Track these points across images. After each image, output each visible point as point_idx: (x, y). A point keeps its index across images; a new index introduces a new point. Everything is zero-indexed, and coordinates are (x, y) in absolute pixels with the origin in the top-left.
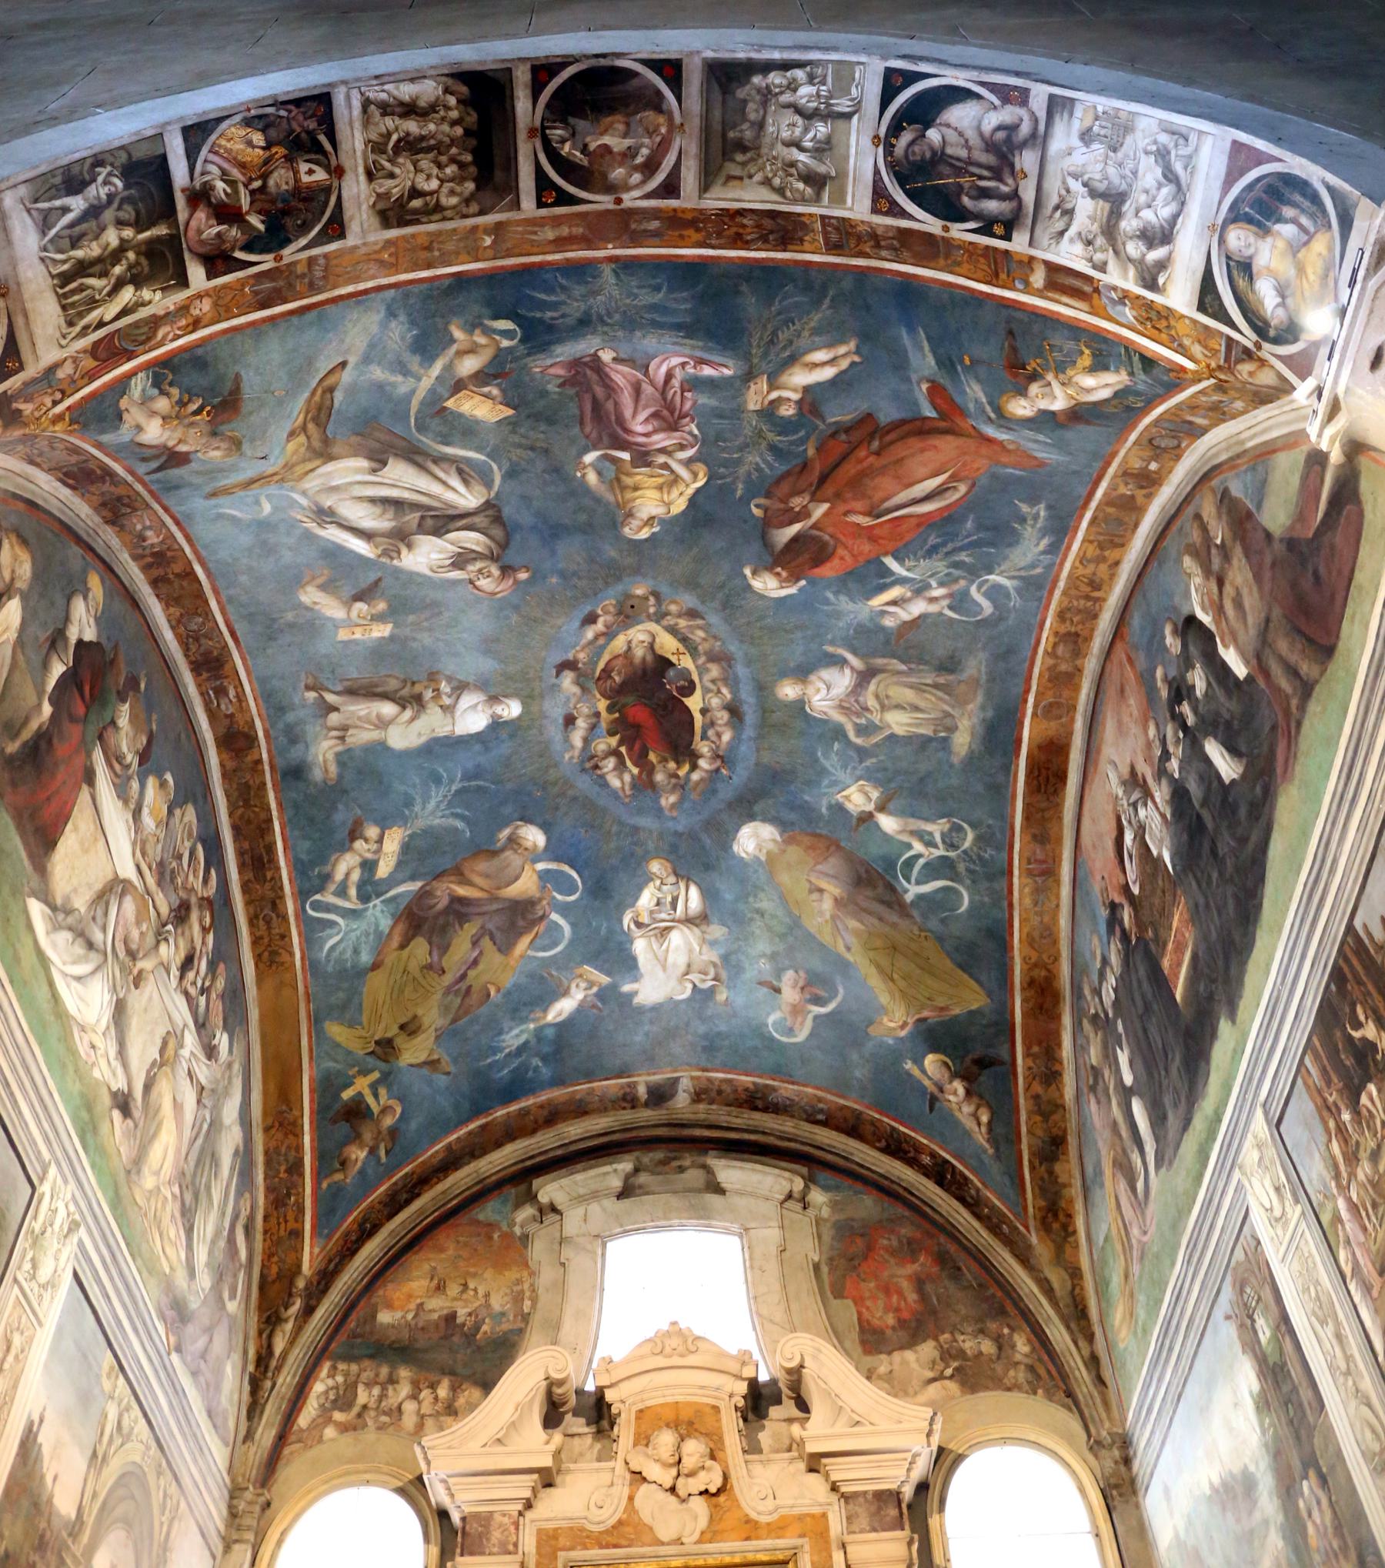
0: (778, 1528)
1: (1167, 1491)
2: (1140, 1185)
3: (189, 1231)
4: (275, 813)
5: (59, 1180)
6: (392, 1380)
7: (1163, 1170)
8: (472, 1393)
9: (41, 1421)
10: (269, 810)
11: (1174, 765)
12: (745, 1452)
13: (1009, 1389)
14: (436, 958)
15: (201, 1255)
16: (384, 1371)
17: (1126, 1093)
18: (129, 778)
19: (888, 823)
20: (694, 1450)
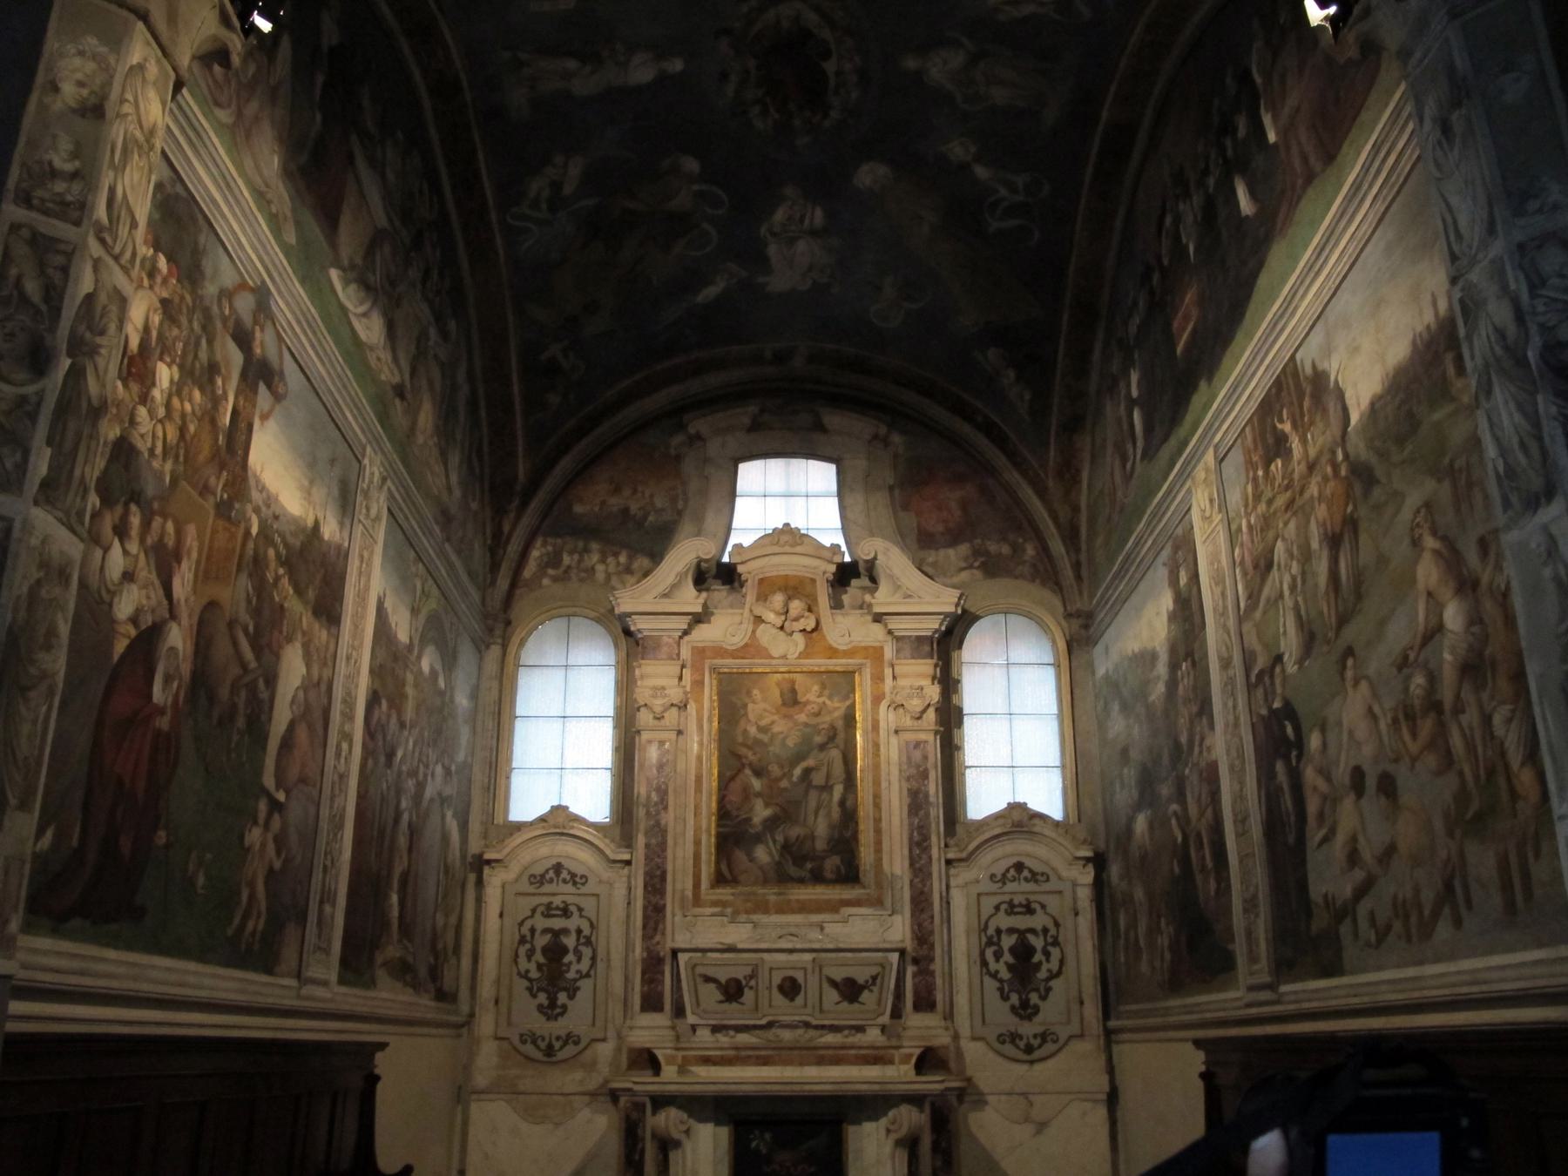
0: (850, 653)
1: (1107, 648)
2: (1129, 466)
3: (445, 464)
5: (373, 455)
6: (586, 550)
7: (1145, 462)
8: (642, 562)
9: (385, 595)
11: (1211, 181)
12: (831, 608)
13: (1016, 578)
15: (454, 478)
16: (581, 544)
17: (1132, 403)
19: (981, 172)
20: (796, 606)
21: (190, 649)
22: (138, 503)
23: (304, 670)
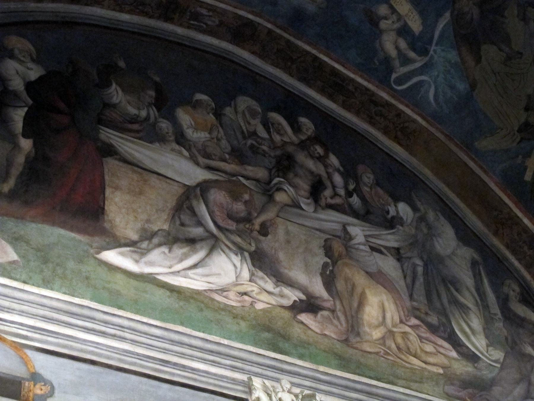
4: (314, 52)
10: (308, 53)
14: (507, 49)
18: (154, 125)
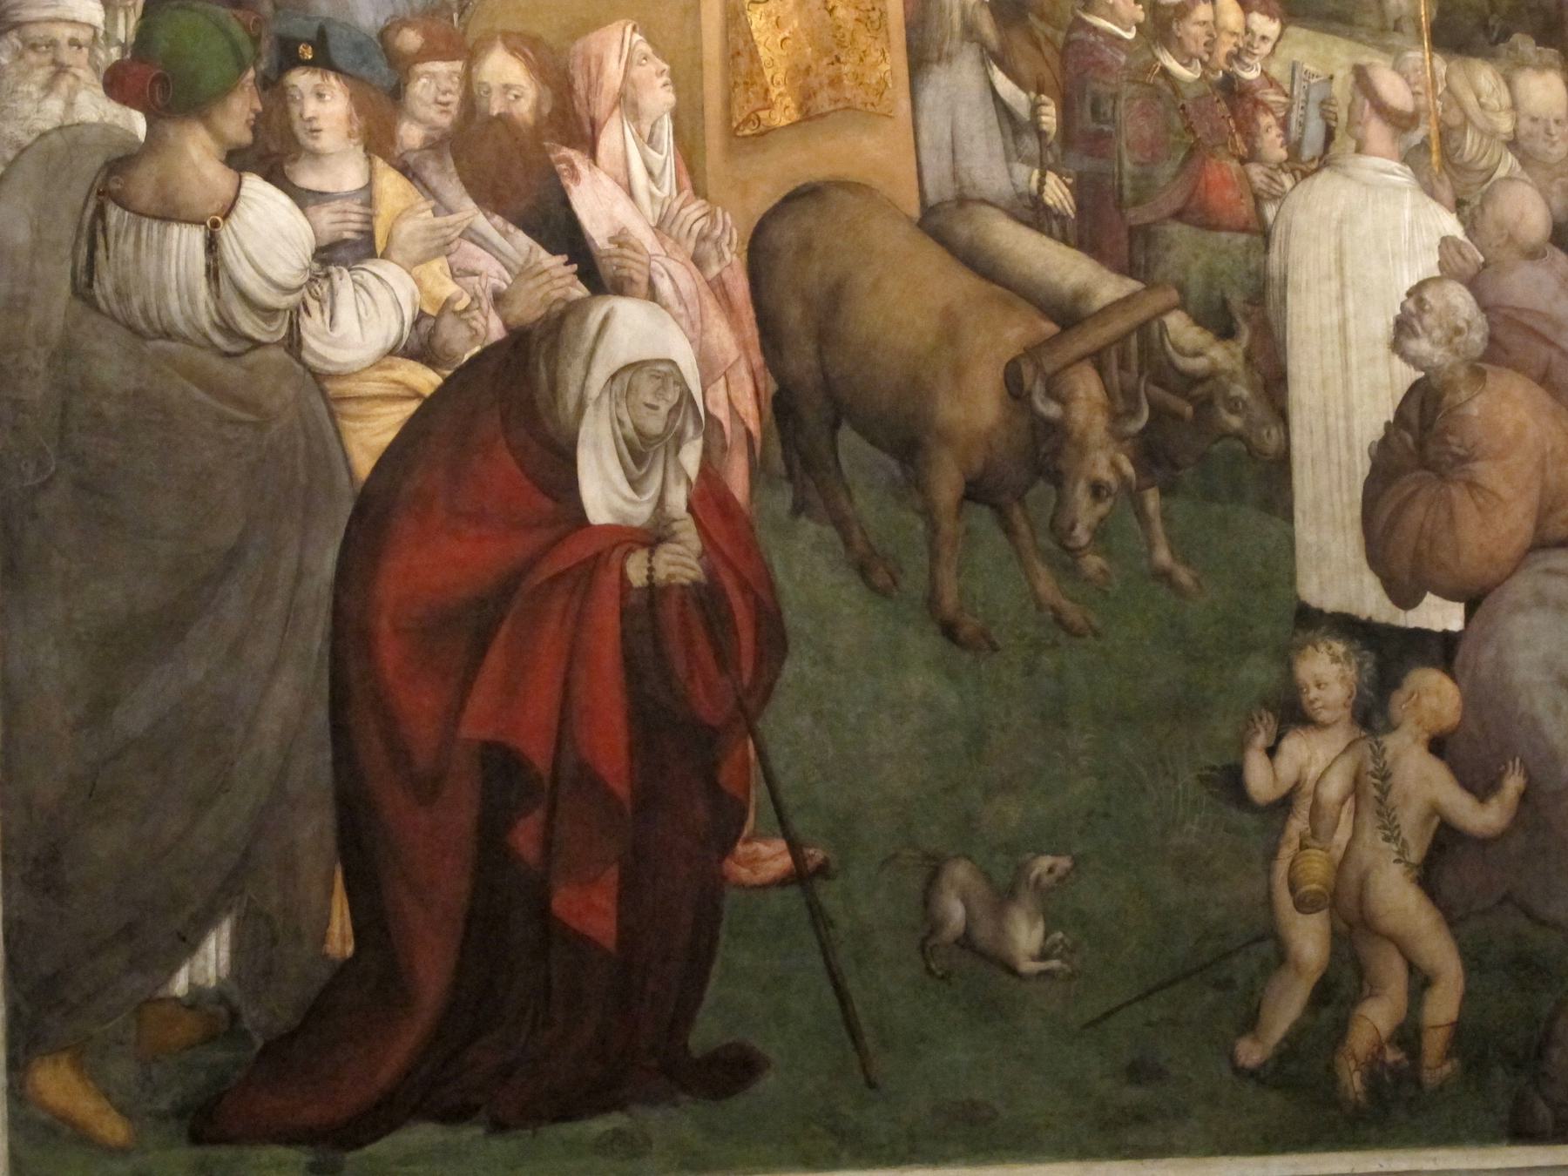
21: (722, 337)
22: (323, 62)
23: (1450, 225)
